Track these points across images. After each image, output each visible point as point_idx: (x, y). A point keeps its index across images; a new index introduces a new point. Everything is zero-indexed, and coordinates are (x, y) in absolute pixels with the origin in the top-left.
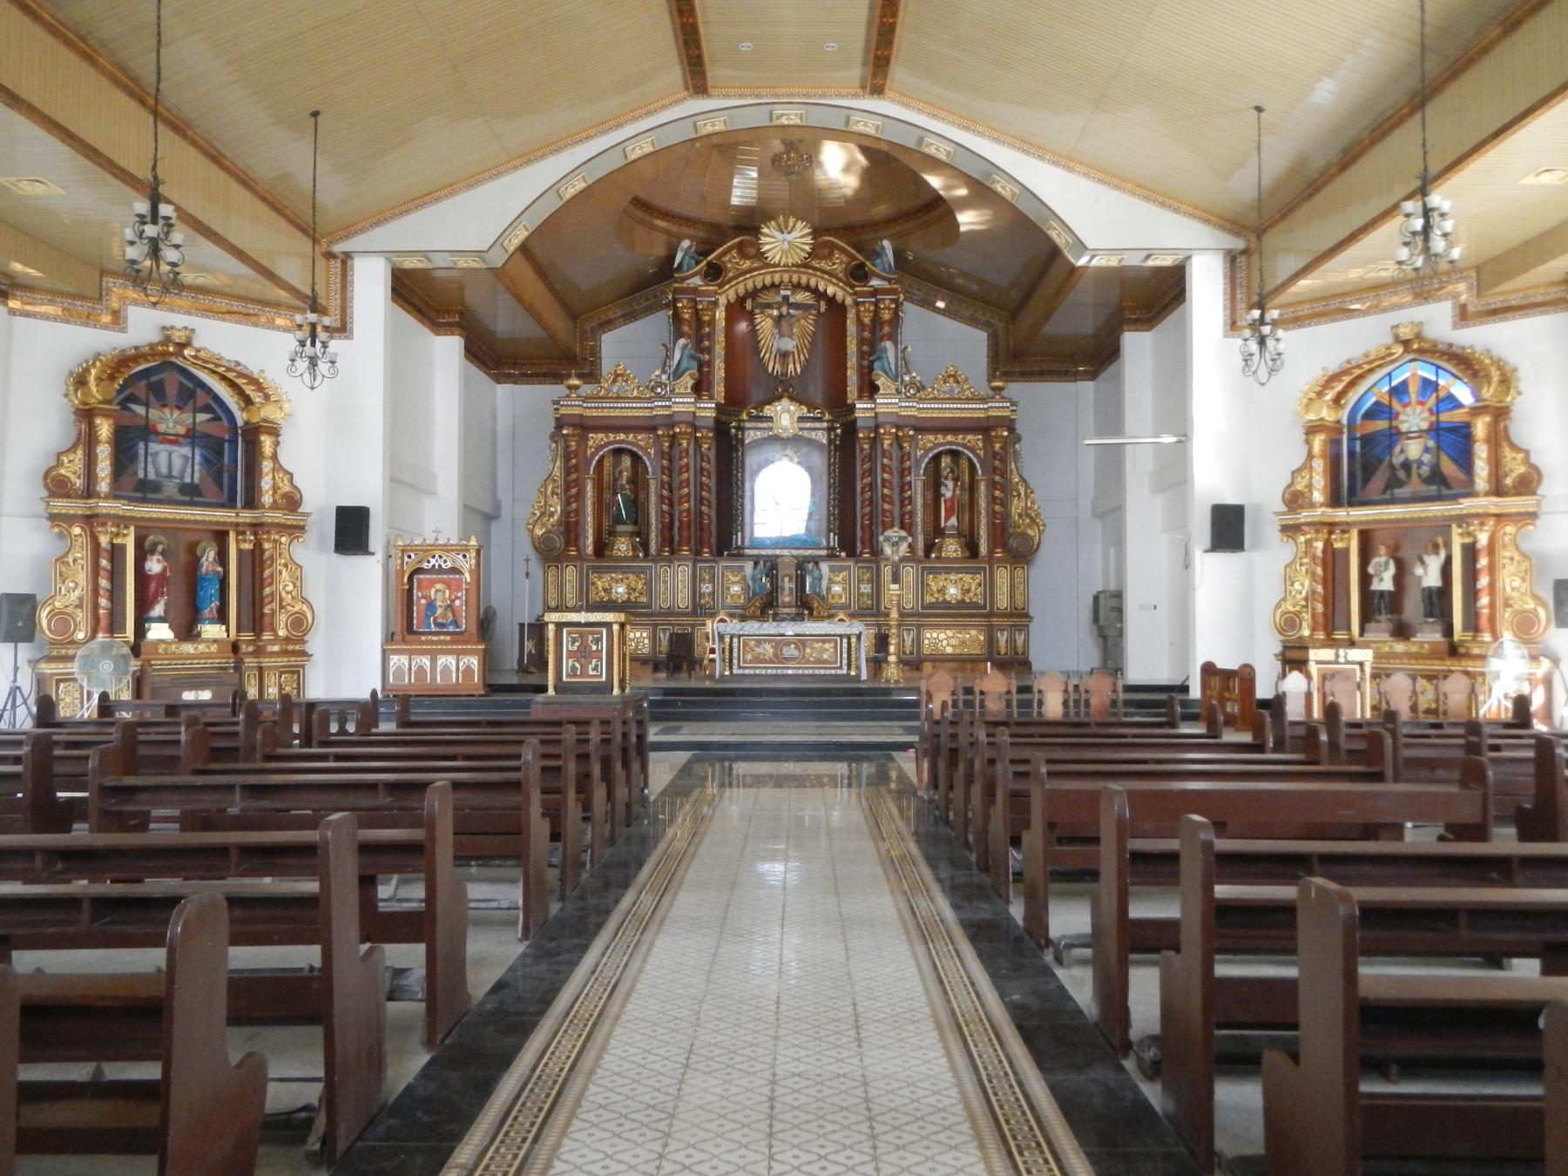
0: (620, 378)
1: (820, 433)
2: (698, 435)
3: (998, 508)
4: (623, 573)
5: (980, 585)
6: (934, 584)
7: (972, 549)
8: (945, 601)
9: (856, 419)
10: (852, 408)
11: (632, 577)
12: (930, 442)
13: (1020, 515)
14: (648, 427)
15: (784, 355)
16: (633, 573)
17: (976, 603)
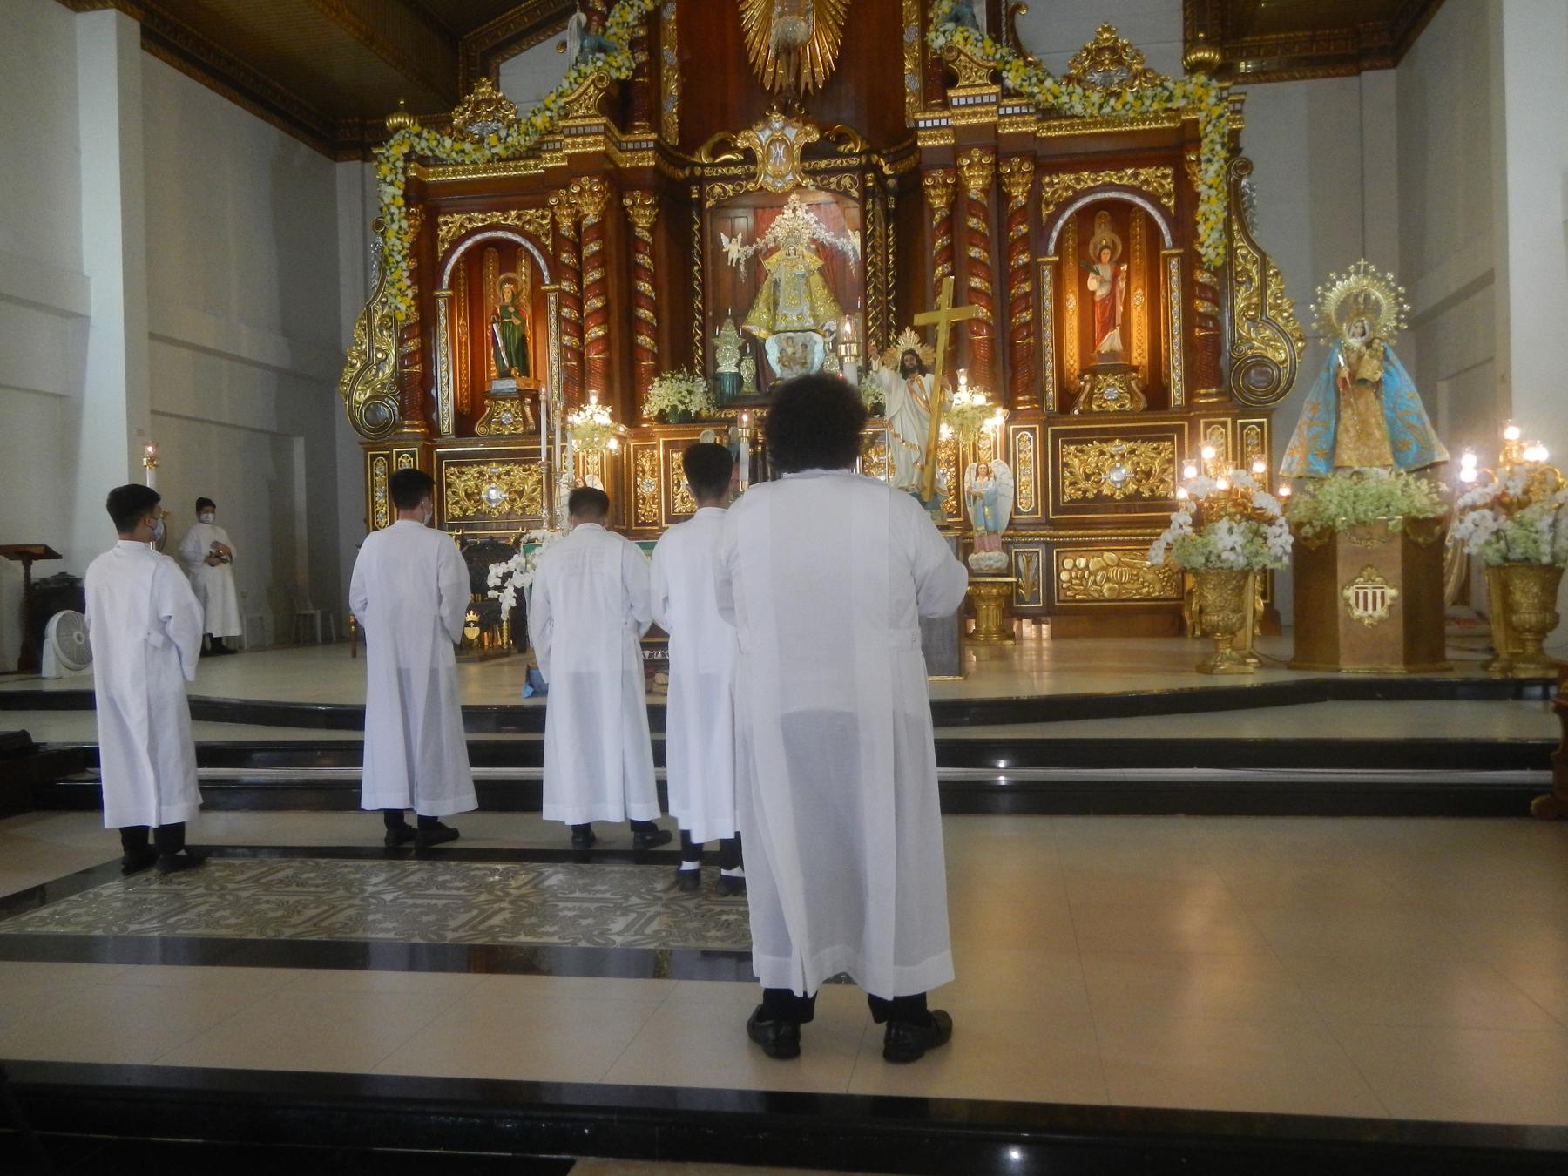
0: (484, 110)
1: (846, 181)
2: (629, 202)
3: (1202, 307)
4: (503, 463)
5: (1170, 461)
6: (1078, 460)
7: (1156, 394)
8: (1099, 496)
9: (920, 149)
10: (913, 133)
11: (517, 470)
12: (1067, 188)
13: (1252, 320)
14: (534, 192)
15: (789, 50)
16: (520, 463)
17: (1166, 498)
